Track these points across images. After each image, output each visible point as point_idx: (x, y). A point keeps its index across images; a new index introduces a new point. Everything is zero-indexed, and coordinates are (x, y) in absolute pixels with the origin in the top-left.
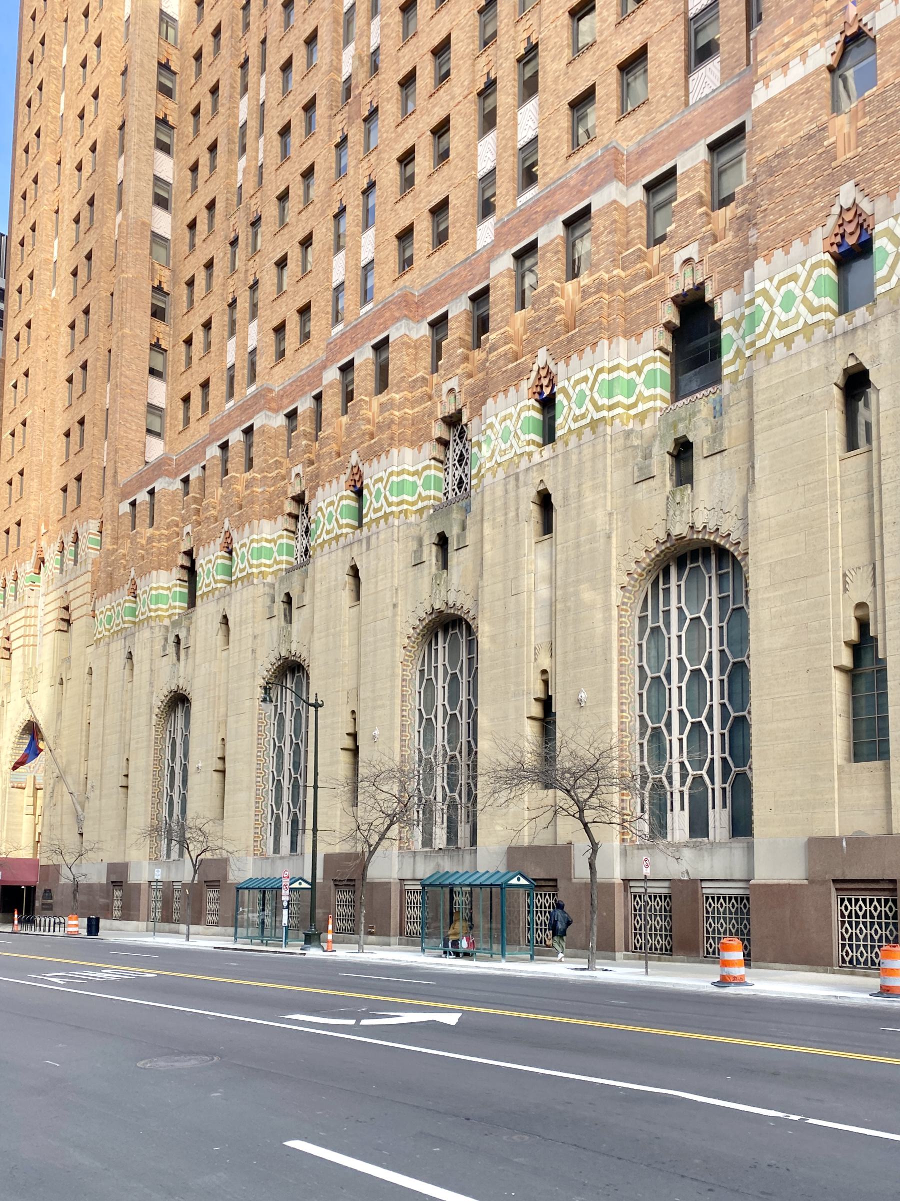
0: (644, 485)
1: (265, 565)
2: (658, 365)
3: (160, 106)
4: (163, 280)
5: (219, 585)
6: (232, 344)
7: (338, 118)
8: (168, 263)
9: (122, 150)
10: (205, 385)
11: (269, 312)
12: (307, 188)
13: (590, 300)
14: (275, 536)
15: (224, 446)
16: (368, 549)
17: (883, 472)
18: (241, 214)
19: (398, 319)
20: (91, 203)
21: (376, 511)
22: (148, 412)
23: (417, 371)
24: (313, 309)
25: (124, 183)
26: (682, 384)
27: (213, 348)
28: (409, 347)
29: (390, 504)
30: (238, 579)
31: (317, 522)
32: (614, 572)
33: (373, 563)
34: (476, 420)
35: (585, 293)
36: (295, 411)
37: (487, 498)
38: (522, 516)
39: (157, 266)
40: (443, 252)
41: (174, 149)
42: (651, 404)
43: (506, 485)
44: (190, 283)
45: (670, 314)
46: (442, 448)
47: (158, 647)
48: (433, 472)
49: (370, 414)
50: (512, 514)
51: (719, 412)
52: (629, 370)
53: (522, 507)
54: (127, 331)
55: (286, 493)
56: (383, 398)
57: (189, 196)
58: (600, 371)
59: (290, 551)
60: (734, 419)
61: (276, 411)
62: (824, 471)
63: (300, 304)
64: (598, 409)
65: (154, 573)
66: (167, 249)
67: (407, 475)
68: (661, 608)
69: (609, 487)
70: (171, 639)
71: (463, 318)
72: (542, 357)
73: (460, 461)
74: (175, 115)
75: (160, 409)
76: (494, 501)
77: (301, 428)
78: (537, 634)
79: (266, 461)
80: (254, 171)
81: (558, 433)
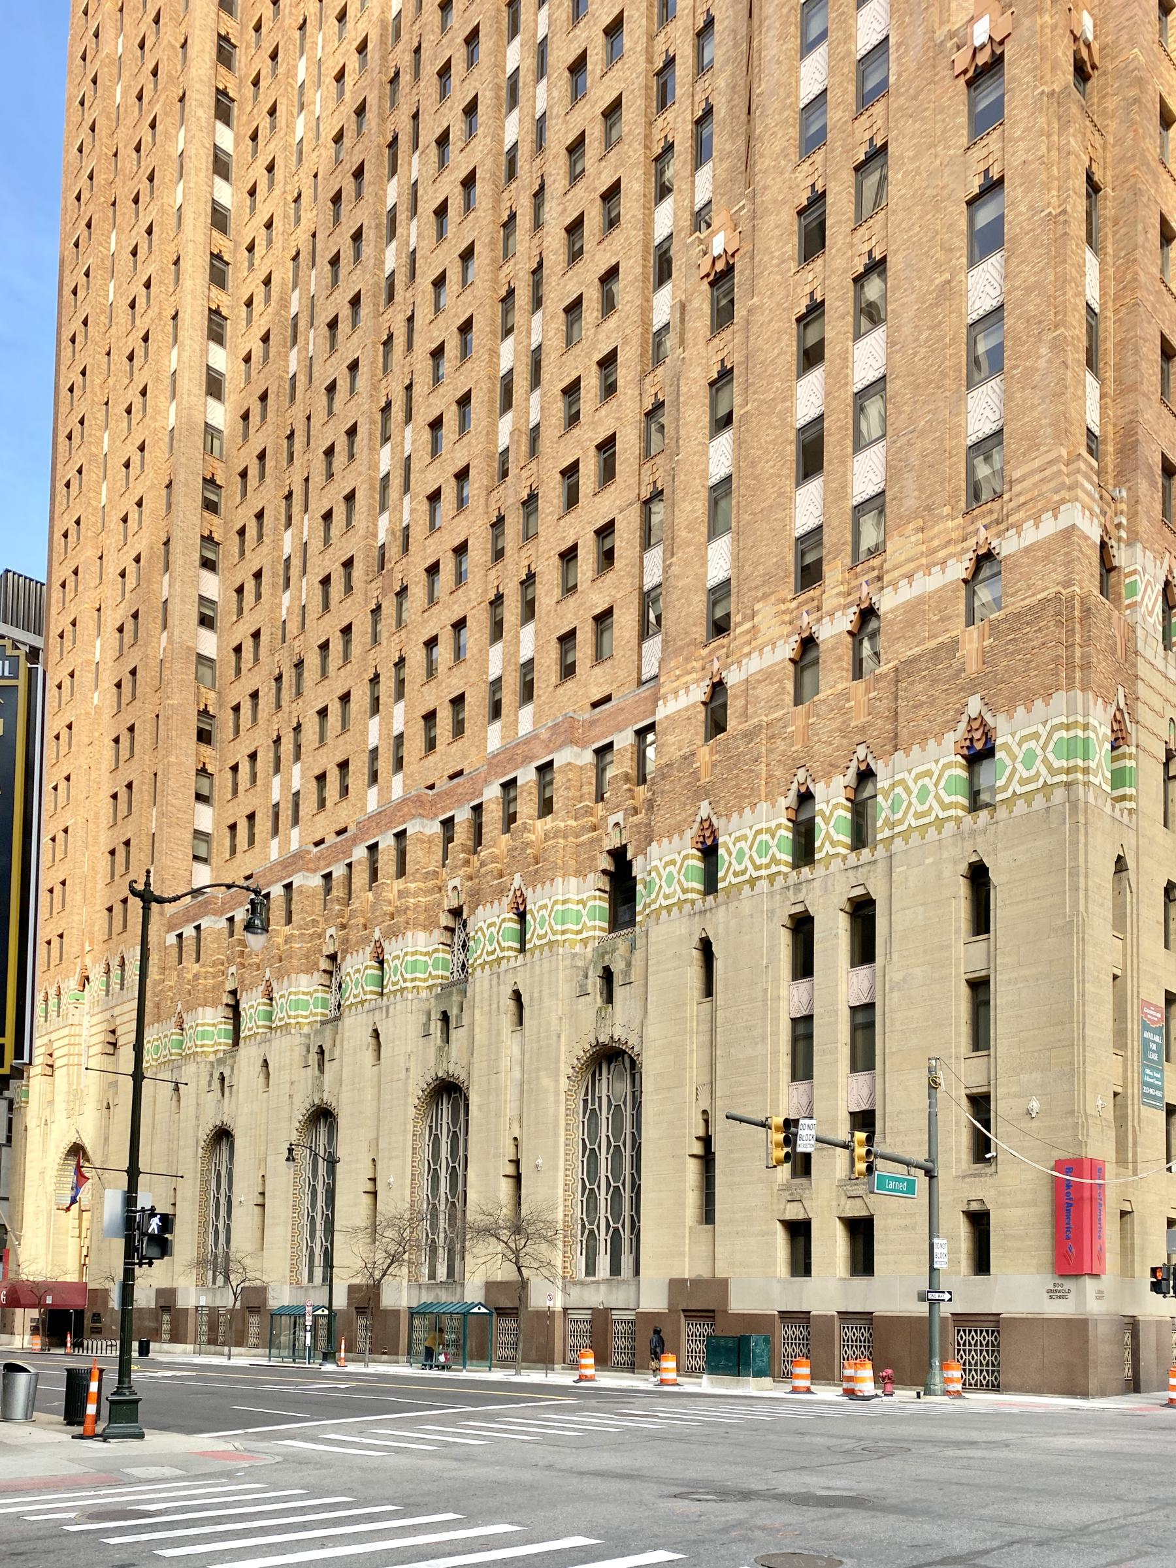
2: (598, 903)
18: (285, 653)
19: (414, 817)
24: (351, 768)
29: (405, 981)
32: (562, 1065)
36: (330, 874)
38: (502, 1009)
48: (441, 955)
49: (390, 896)
50: (494, 1006)
51: (633, 948)
58: (556, 902)
64: (554, 933)
66: (212, 668)
67: (419, 952)
73: (464, 945)
78: (510, 1108)
80: (297, 610)
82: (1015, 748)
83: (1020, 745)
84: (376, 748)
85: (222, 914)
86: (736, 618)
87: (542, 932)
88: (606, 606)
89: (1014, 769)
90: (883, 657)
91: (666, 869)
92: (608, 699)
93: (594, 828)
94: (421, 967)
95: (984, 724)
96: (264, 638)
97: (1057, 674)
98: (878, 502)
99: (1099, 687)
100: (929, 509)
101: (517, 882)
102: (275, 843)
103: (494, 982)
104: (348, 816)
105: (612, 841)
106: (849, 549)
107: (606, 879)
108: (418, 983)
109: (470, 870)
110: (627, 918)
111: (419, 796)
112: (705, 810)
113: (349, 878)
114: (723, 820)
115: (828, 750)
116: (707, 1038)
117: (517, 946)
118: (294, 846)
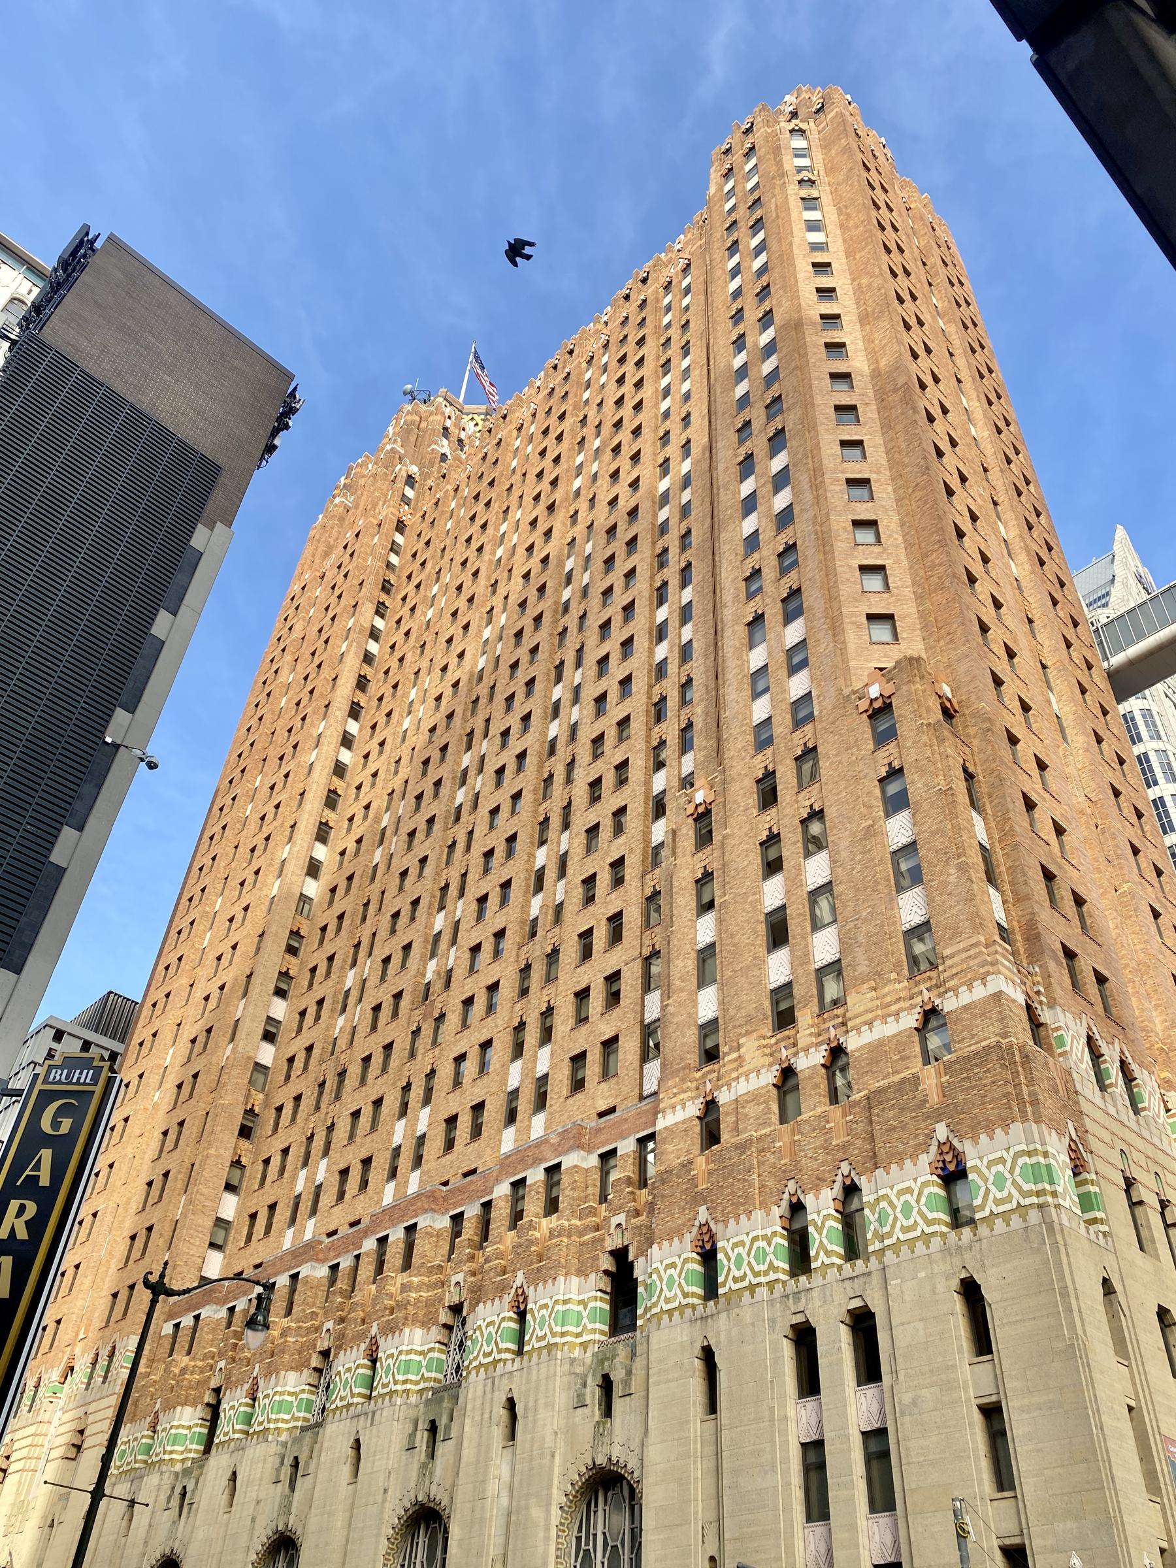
1: (283, 1421)
2: (599, 1304)
5: (236, 1436)
14: (298, 1389)
16: (372, 1424)
19: (426, 1211)
21: (385, 1386)
29: (396, 1382)
33: (374, 1440)
37: (470, 1396)
38: (495, 1419)
40: (476, 1144)
43: (485, 1386)
47: (163, 1497)
48: (436, 1355)
49: (393, 1290)
50: (486, 1416)
58: (557, 1302)
64: (554, 1335)
65: (179, 1408)
70: (178, 1490)
71: (474, 1220)
72: (520, 1279)
73: (461, 1345)
79: (304, 1311)
81: (526, 1348)
82: (985, 1170)
83: (988, 1168)
84: (399, 1147)
85: (224, 1303)
86: (724, 1049)
87: (541, 1334)
88: (612, 1034)
89: (987, 1191)
90: (855, 1087)
91: (667, 1271)
92: (613, 1110)
94: (414, 1367)
95: (952, 1148)
97: (1011, 1108)
98: (836, 967)
99: (1050, 1120)
100: (878, 974)
101: (520, 1279)
102: (290, 1233)
104: (364, 1209)
105: (614, 1242)
106: (816, 1000)
107: (607, 1280)
108: (409, 1386)
109: (473, 1266)
110: (627, 1322)
111: (433, 1192)
112: (703, 1214)
113: (355, 1269)
114: (721, 1225)
115: (815, 1165)
117: (514, 1347)
118: (308, 1236)
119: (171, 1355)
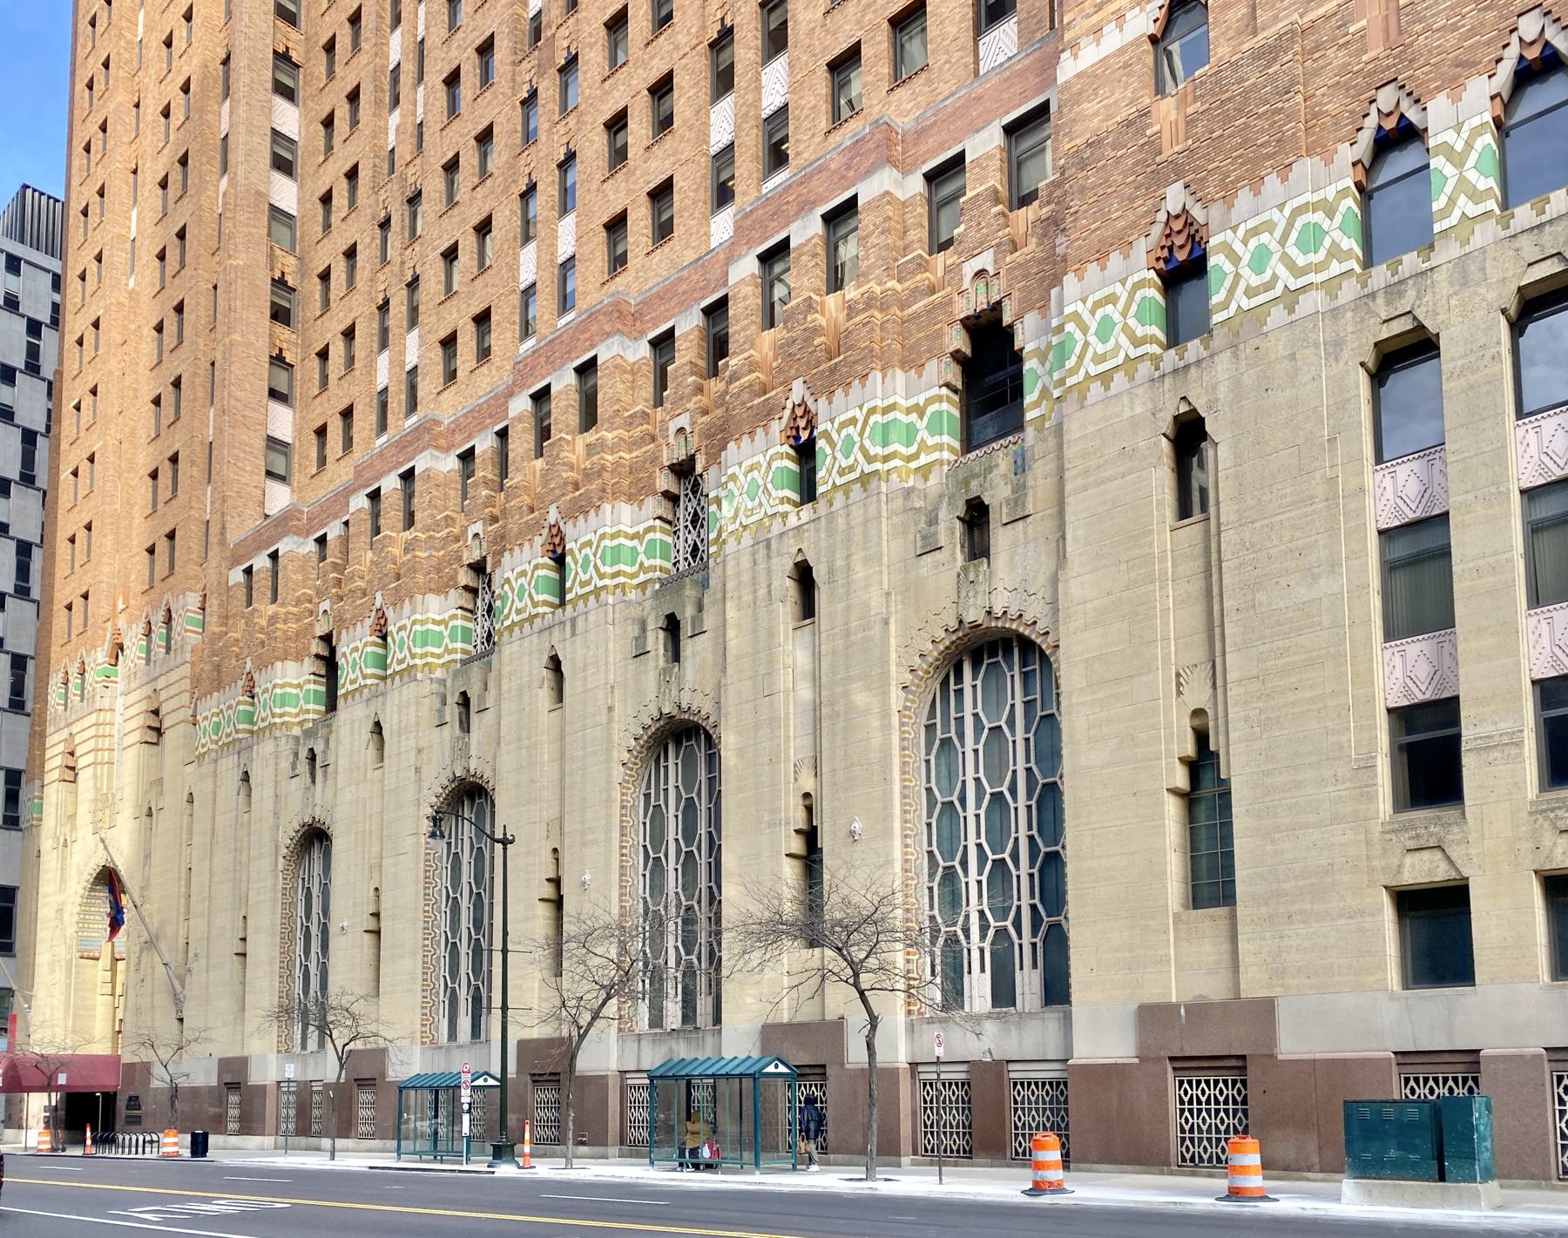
0: (928, 558)
1: (433, 655)
2: (945, 406)
3: (279, 36)
4: (286, 270)
5: (369, 682)
6: (383, 360)
7: (524, 65)
8: (294, 249)
9: (227, 93)
10: (347, 414)
11: (433, 319)
12: (484, 157)
13: (858, 319)
14: (446, 616)
15: (375, 496)
16: (573, 634)
17: (1223, 546)
19: (608, 335)
20: (184, 161)
21: (583, 584)
22: (268, 447)
23: (635, 403)
24: (494, 318)
25: (230, 137)
26: (976, 429)
27: (357, 365)
28: (625, 372)
29: (602, 576)
30: (395, 673)
31: (503, 598)
32: (893, 668)
33: (580, 652)
34: (713, 470)
35: (851, 309)
37: (730, 571)
38: (776, 595)
39: (278, 252)
40: (666, 249)
41: (301, 94)
42: (936, 456)
43: (753, 554)
44: (325, 276)
45: (958, 340)
46: (670, 505)
48: (658, 535)
49: (573, 459)
50: (762, 592)
51: (1021, 466)
52: (908, 411)
53: (776, 584)
54: (237, 337)
55: (460, 559)
56: (590, 437)
57: (322, 158)
58: (872, 411)
59: (467, 635)
60: (1040, 477)
61: (447, 450)
62: (1151, 543)
63: (477, 309)
64: (870, 459)
65: (279, 664)
66: (292, 228)
67: (623, 538)
68: (953, 714)
69: (885, 559)
71: (695, 336)
72: (798, 391)
73: (694, 522)
74: (301, 50)
75: (286, 445)
76: (738, 574)
77: (479, 474)
79: (432, 516)
80: (411, 129)
81: (820, 490)
93: (932, 290)
94: (626, 555)
96: (363, 174)
101: (798, 391)
103: (762, 552)
116: (1197, 585)
119: (249, 603)
